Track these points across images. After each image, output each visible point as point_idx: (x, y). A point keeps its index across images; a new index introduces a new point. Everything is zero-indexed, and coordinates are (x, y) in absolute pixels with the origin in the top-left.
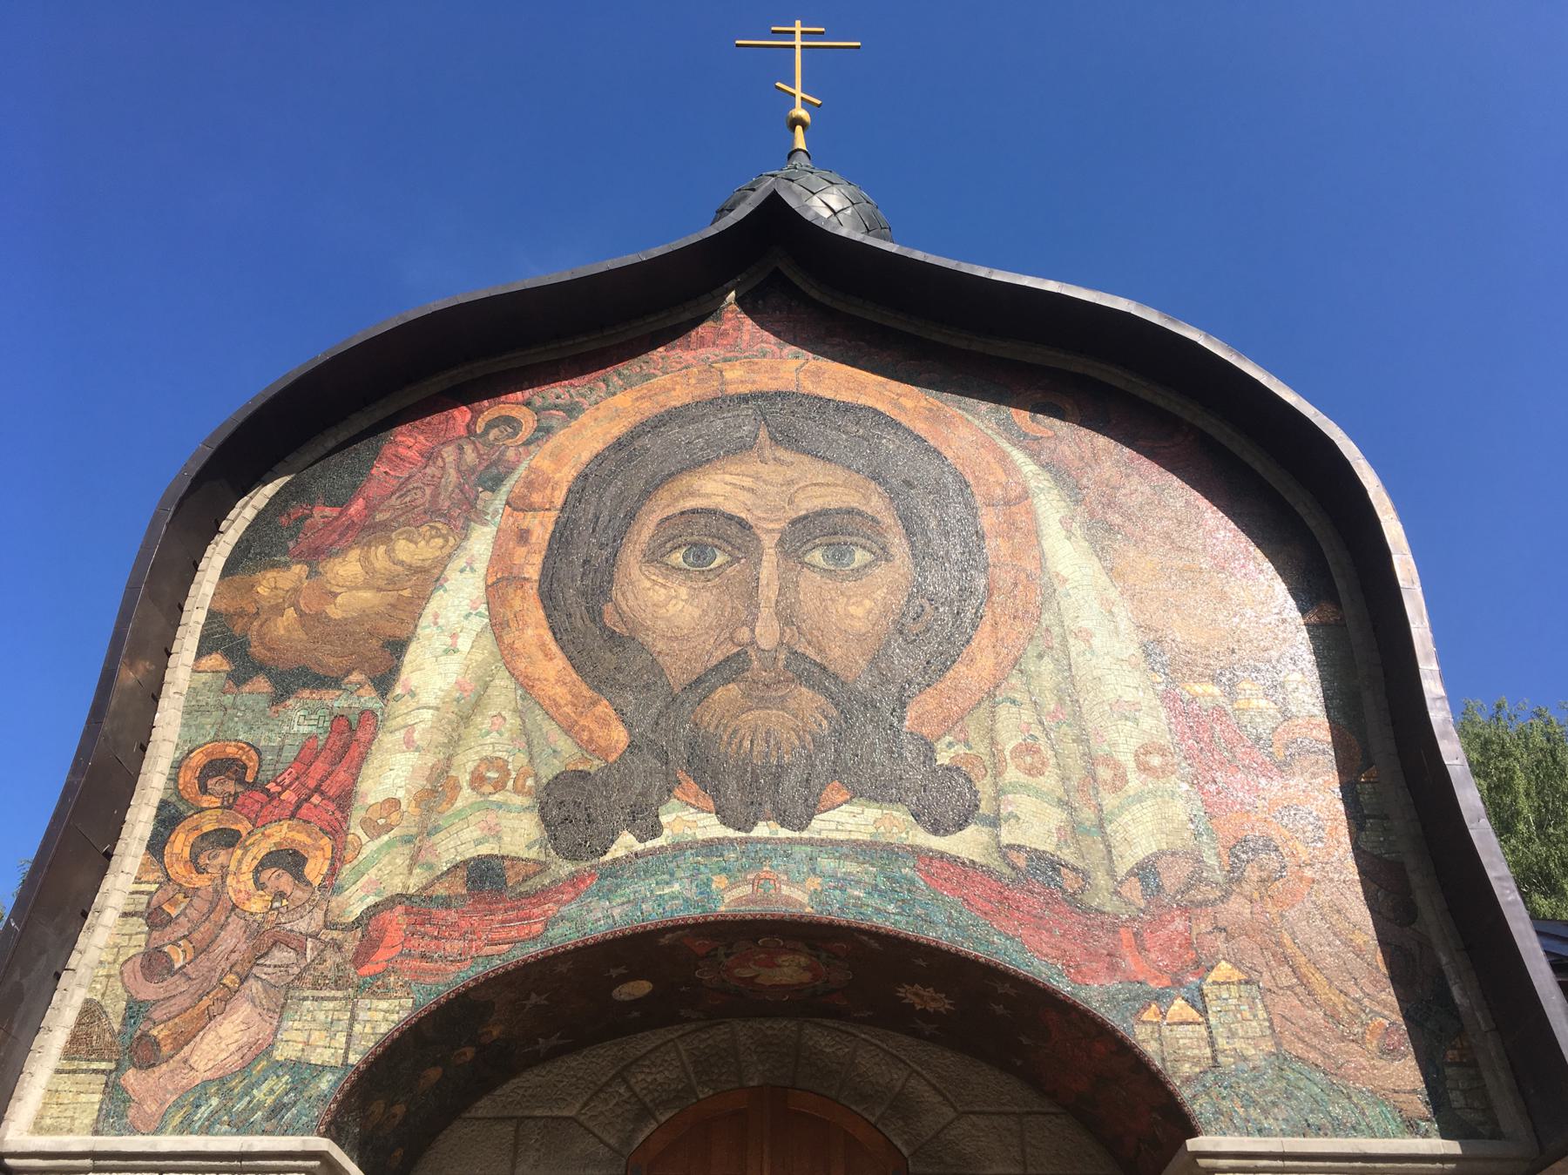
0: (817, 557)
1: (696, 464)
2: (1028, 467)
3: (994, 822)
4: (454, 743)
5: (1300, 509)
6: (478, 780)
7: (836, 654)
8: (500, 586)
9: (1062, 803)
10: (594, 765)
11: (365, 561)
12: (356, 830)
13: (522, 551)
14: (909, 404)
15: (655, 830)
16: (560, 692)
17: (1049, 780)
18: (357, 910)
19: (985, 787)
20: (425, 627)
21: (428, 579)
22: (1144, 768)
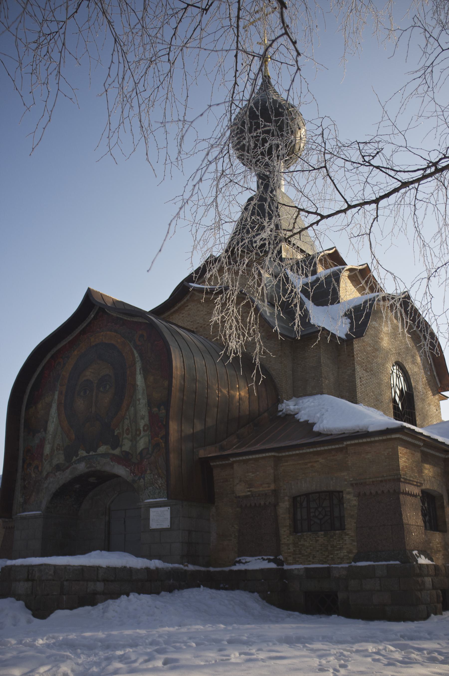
0: (101, 389)
2: (136, 355)
3: (121, 447)
9: (131, 441)
12: (44, 461)
14: (119, 340)
15: (77, 456)
17: (129, 436)
18: (45, 475)
19: (121, 439)
21: (49, 406)
22: (144, 430)
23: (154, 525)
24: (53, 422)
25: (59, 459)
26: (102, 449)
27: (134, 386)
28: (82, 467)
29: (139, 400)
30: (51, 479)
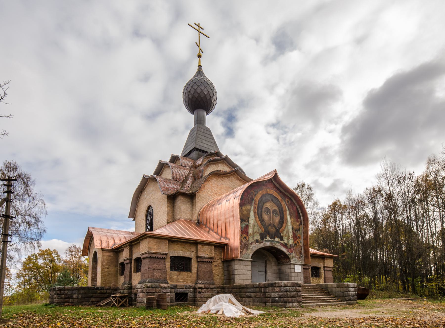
1: (266, 202)
2: (287, 208)
3: (284, 241)
4: (254, 229)
5: (301, 216)
6: (256, 232)
7: (276, 225)
8: (255, 213)
9: (287, 240)
10: (262, 232)
11: (245, 208)
12: (249, 236)
13: (255, 209)
15: (266, 239)
16: (260, 225)
17: (286, 238)
20: (250, 217)
21: (249, 211)
23: (296, 271)
24: (252, 219)
25: (258, 237)
26: (277, 239)
27: (287, 219)
28: (268, 244)
29: (289, 226)
30: (254, 246)
